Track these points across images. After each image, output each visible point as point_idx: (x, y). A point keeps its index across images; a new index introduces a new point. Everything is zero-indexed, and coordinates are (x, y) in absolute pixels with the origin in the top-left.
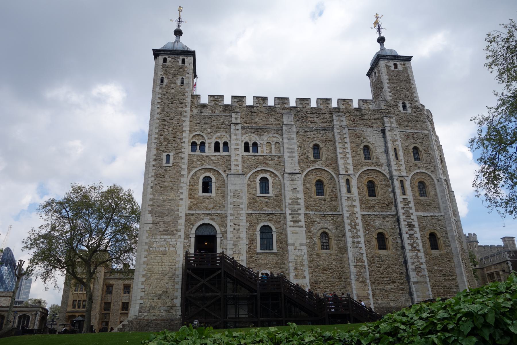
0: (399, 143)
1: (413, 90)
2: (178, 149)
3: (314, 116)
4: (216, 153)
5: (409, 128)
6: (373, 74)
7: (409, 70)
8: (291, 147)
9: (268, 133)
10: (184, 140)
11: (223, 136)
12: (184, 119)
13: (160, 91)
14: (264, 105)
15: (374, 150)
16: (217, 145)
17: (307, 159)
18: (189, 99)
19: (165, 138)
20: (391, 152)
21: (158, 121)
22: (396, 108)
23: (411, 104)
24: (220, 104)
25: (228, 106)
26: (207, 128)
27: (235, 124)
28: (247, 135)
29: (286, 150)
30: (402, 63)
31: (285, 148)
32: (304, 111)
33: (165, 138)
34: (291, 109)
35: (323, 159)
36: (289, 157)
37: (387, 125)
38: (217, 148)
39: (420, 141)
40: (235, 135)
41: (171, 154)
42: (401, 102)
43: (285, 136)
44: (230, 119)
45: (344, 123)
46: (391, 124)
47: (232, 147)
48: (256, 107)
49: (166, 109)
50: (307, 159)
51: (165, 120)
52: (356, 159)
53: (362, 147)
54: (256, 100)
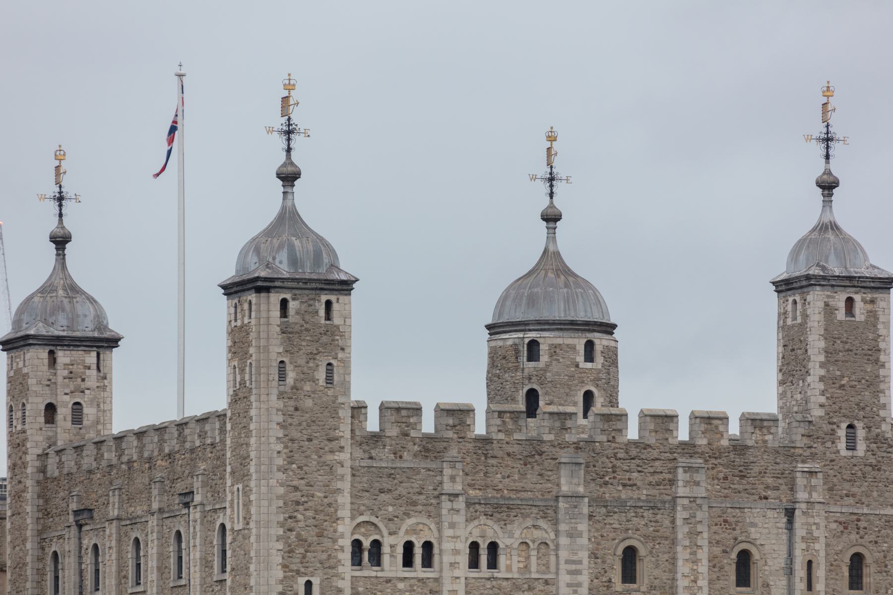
0: (820, 546)
1: (882, 386)
2: (330, 566)
3: (633, 466)
4: (407, 573)
5: (851, 500)
6: (791, 299)
7: (882, 318)
8: (575, 558)
9: (525, 516)
10: (341, 542)
11: (421, 526)
12: (339, 485)
13: (280, 404)
14: (517, 436)
15: (760, 563)
16: (409, 547)
17: (608, 587)
18: (345, 430)
19: (301, 540)
20: (800, 572)
21: (281, 490)
22: (829, 444)
23: (869, 428)
24: (413, 434)
25: (428, 438)
26: (385, 504)
27: (450, 495)
28: (476, 522)
29: (563, 567)
30: (869, 296)
31: (562, 561)
32: (610, 452)
33: (298, 536)
34: (577, 447)
35: (644, 588)
36: (569, 585)
37: (802, 495)
38: (408, 561)
39: (872, 538)
40: (452, 525)
41: (316, 581)
42: (844, 426)
43: (563, 527)
44: (439, 478)
45: (701, 492)
46: (810, 494)
47: (444, 556)
48: (499, 441)
49: (297, 456)
50: (608, 587)
51: (296, 489)
52: (717, 586)
53: (734, 556)
54: (498, 422)
